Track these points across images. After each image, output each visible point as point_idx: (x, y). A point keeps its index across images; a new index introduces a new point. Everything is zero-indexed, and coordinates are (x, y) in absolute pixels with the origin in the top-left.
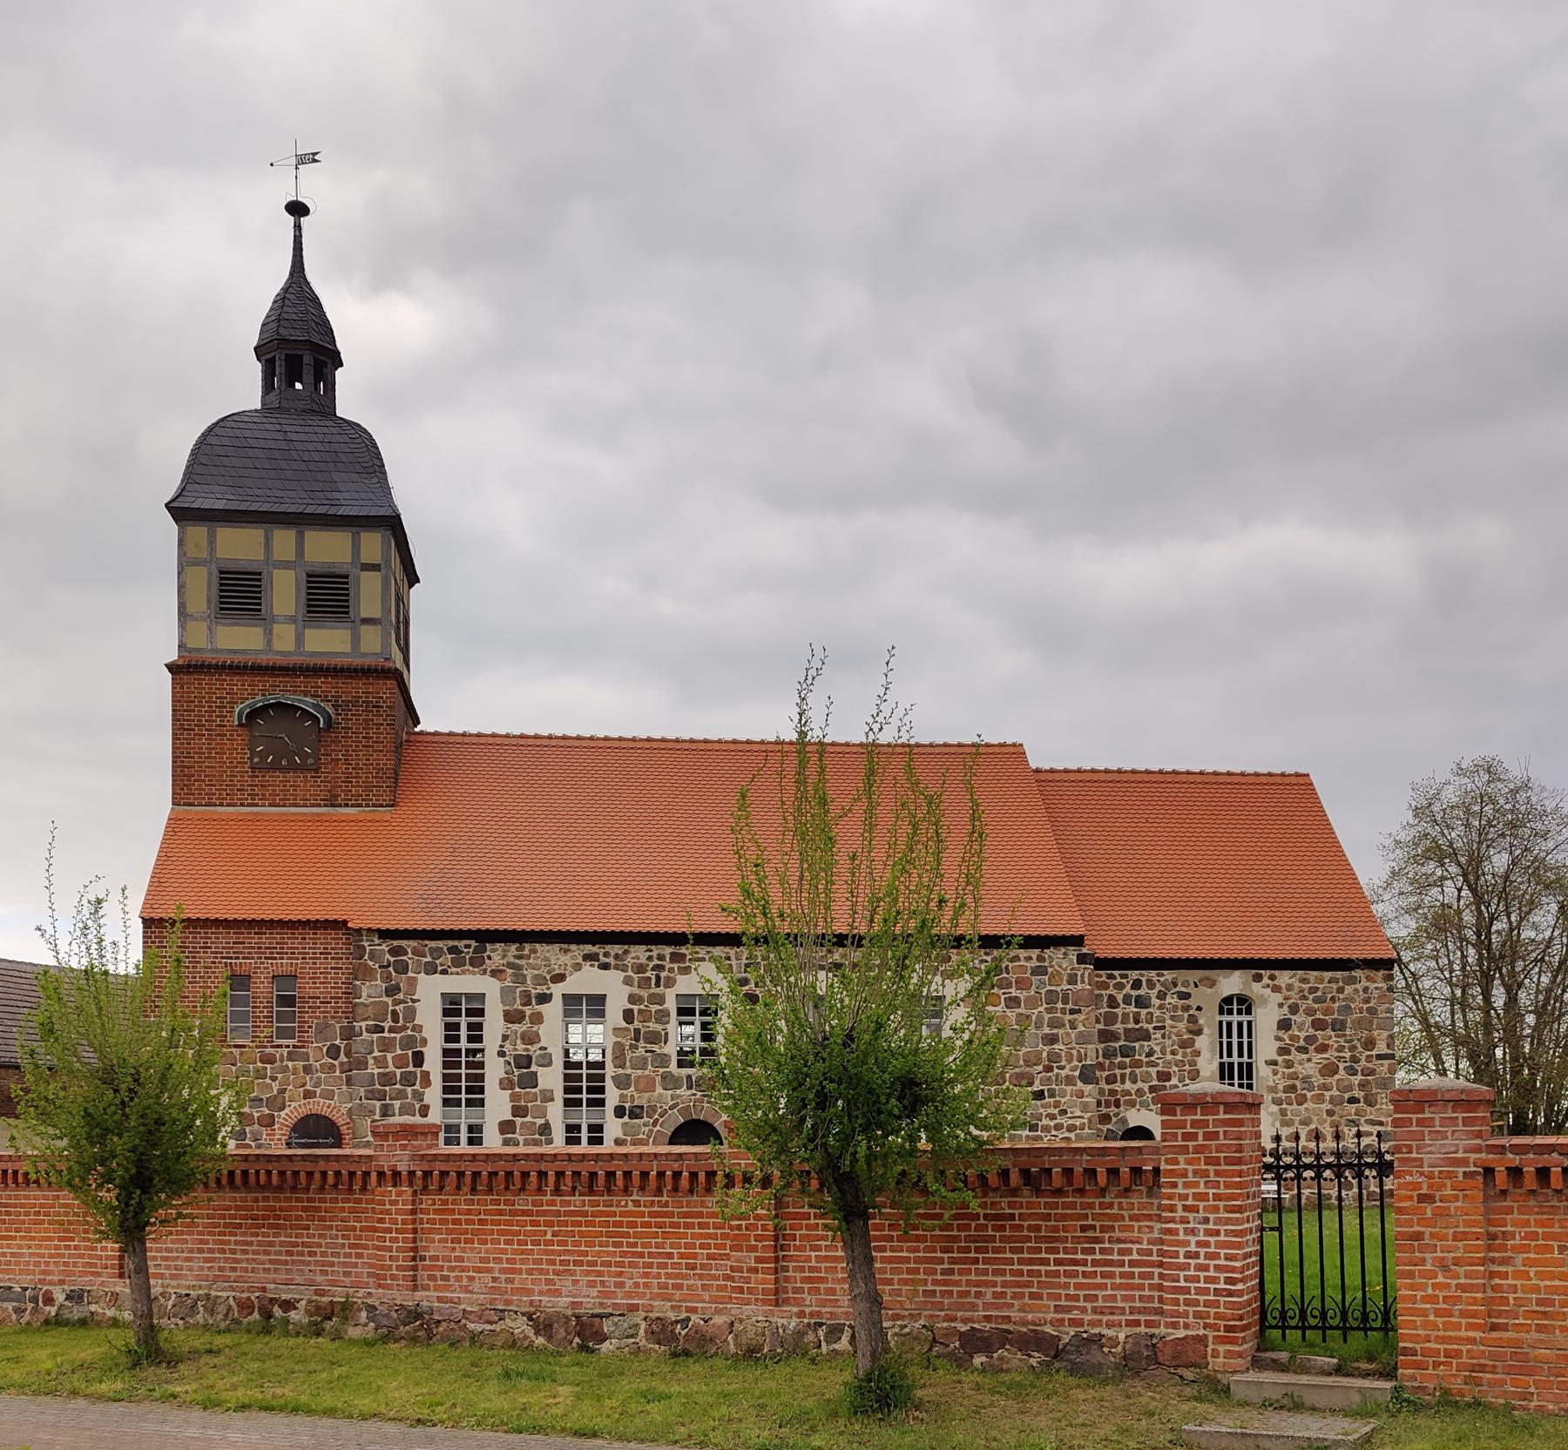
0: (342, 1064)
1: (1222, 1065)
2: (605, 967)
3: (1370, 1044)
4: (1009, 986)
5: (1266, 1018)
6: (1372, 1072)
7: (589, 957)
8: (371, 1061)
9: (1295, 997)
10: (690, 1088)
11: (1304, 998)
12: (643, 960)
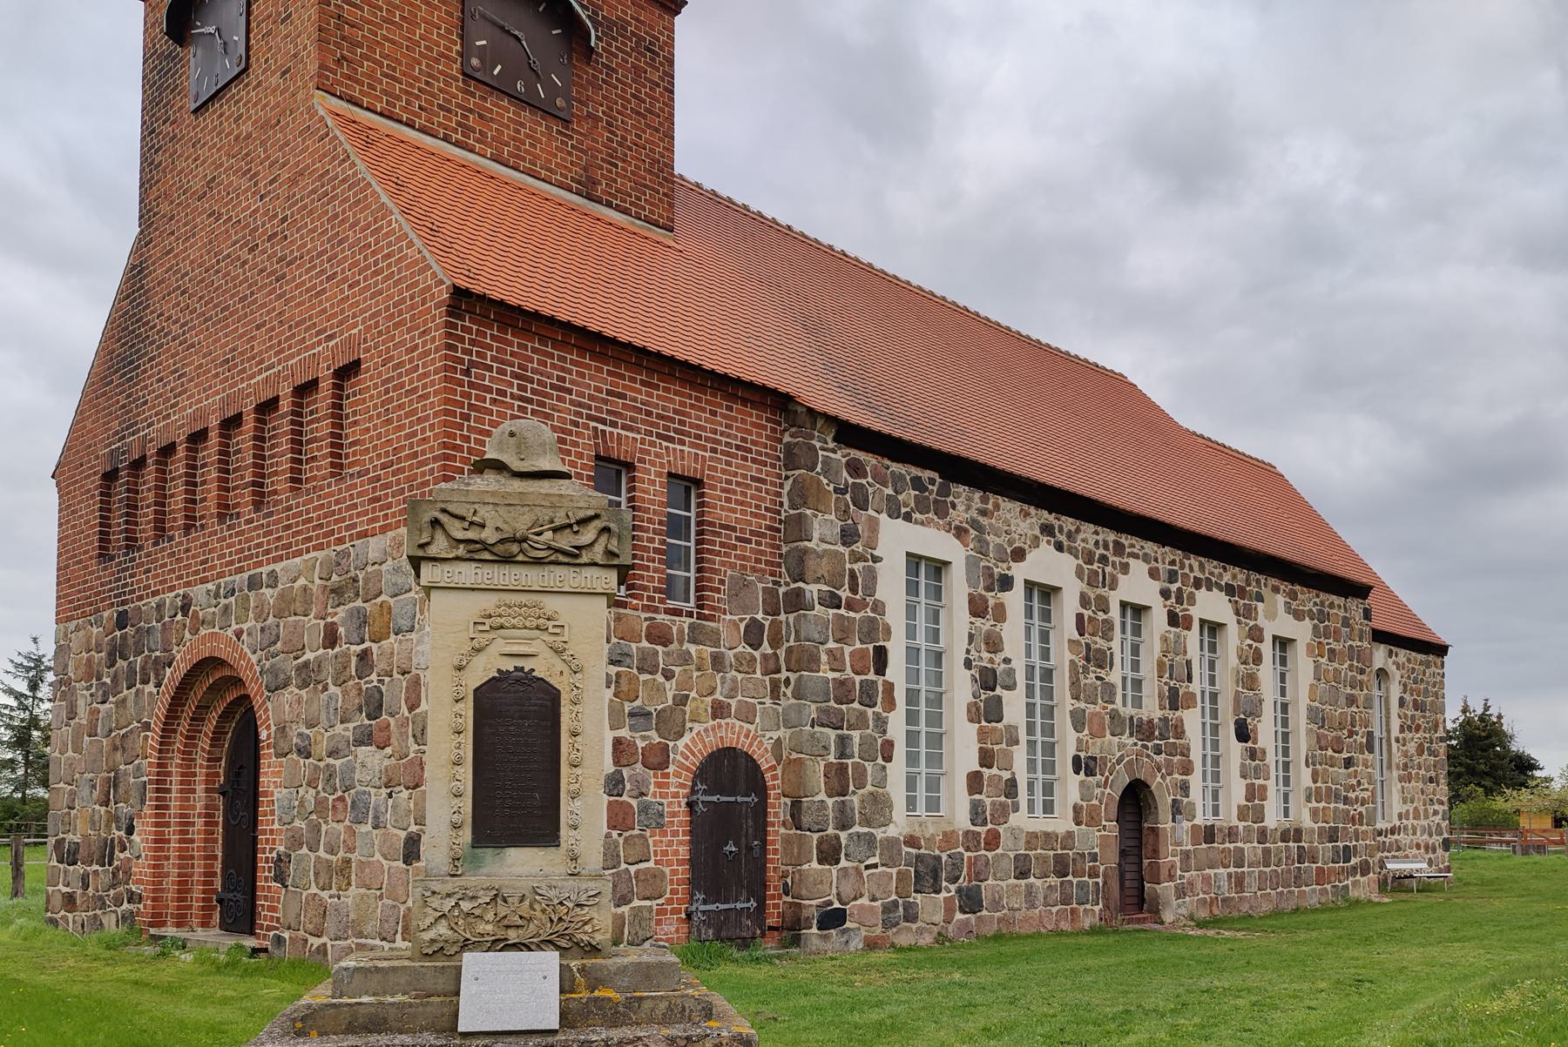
0: (764, 656)
7: (1047, 530)
8: (824, 658)
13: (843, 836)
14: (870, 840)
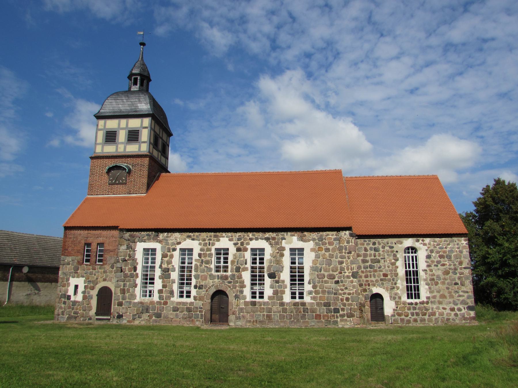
1: (406, 272)
2: (193, 239)
3: (461, 263)
4: (326, 244)
5: (422, 255)
6: (462, 273)
7: (189, 237)
9: (432, 248)
10: (218, 279)
11: (435, 247)
12: (205, 237)
13: (124, 301)
14: (130, 303)
